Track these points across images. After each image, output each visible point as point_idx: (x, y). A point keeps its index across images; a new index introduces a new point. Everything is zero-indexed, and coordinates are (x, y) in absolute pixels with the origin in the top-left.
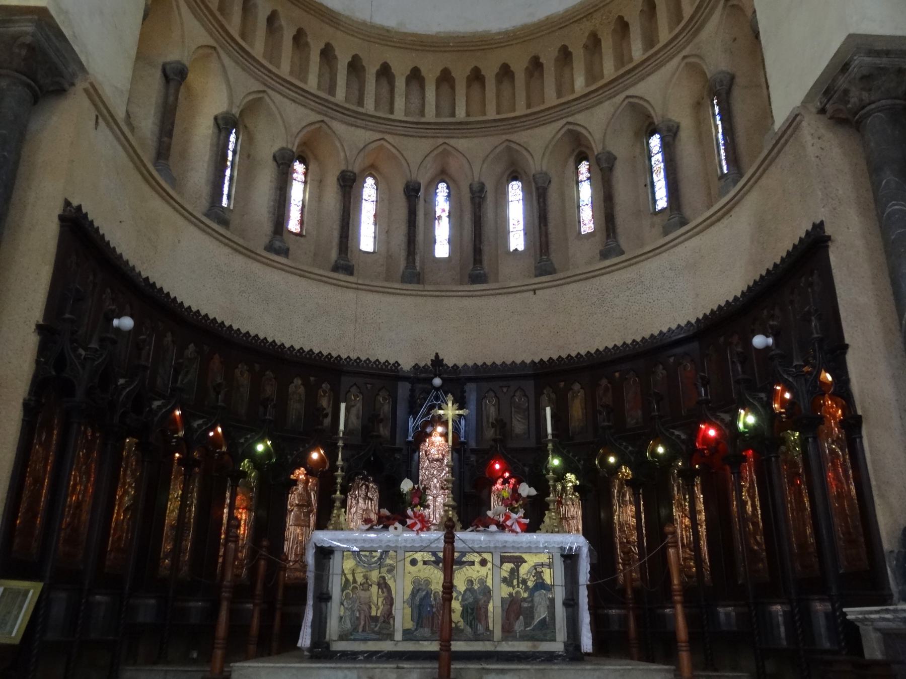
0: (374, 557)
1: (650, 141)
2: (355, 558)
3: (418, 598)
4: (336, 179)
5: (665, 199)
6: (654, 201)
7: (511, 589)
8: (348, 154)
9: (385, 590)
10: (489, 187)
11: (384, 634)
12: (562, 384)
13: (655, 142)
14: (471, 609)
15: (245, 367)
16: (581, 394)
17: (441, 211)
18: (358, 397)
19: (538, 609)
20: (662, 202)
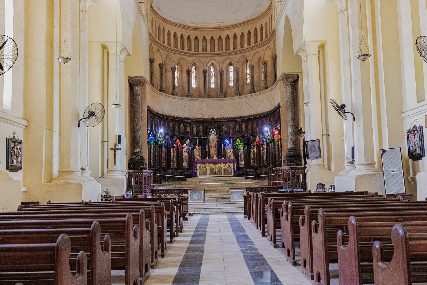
8: (188, 64)
10: (224, 69)
16: (245, 125)
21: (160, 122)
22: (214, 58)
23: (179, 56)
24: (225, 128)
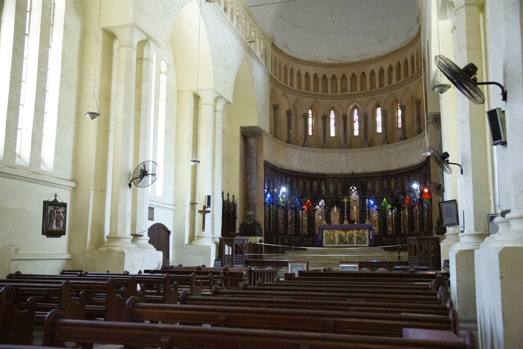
3: (340, 237)
10: (369, 112)
16: (394, 181)
21: (286, 180)
22: (356, 99)
23: (312, 100)
24: (370, 186)
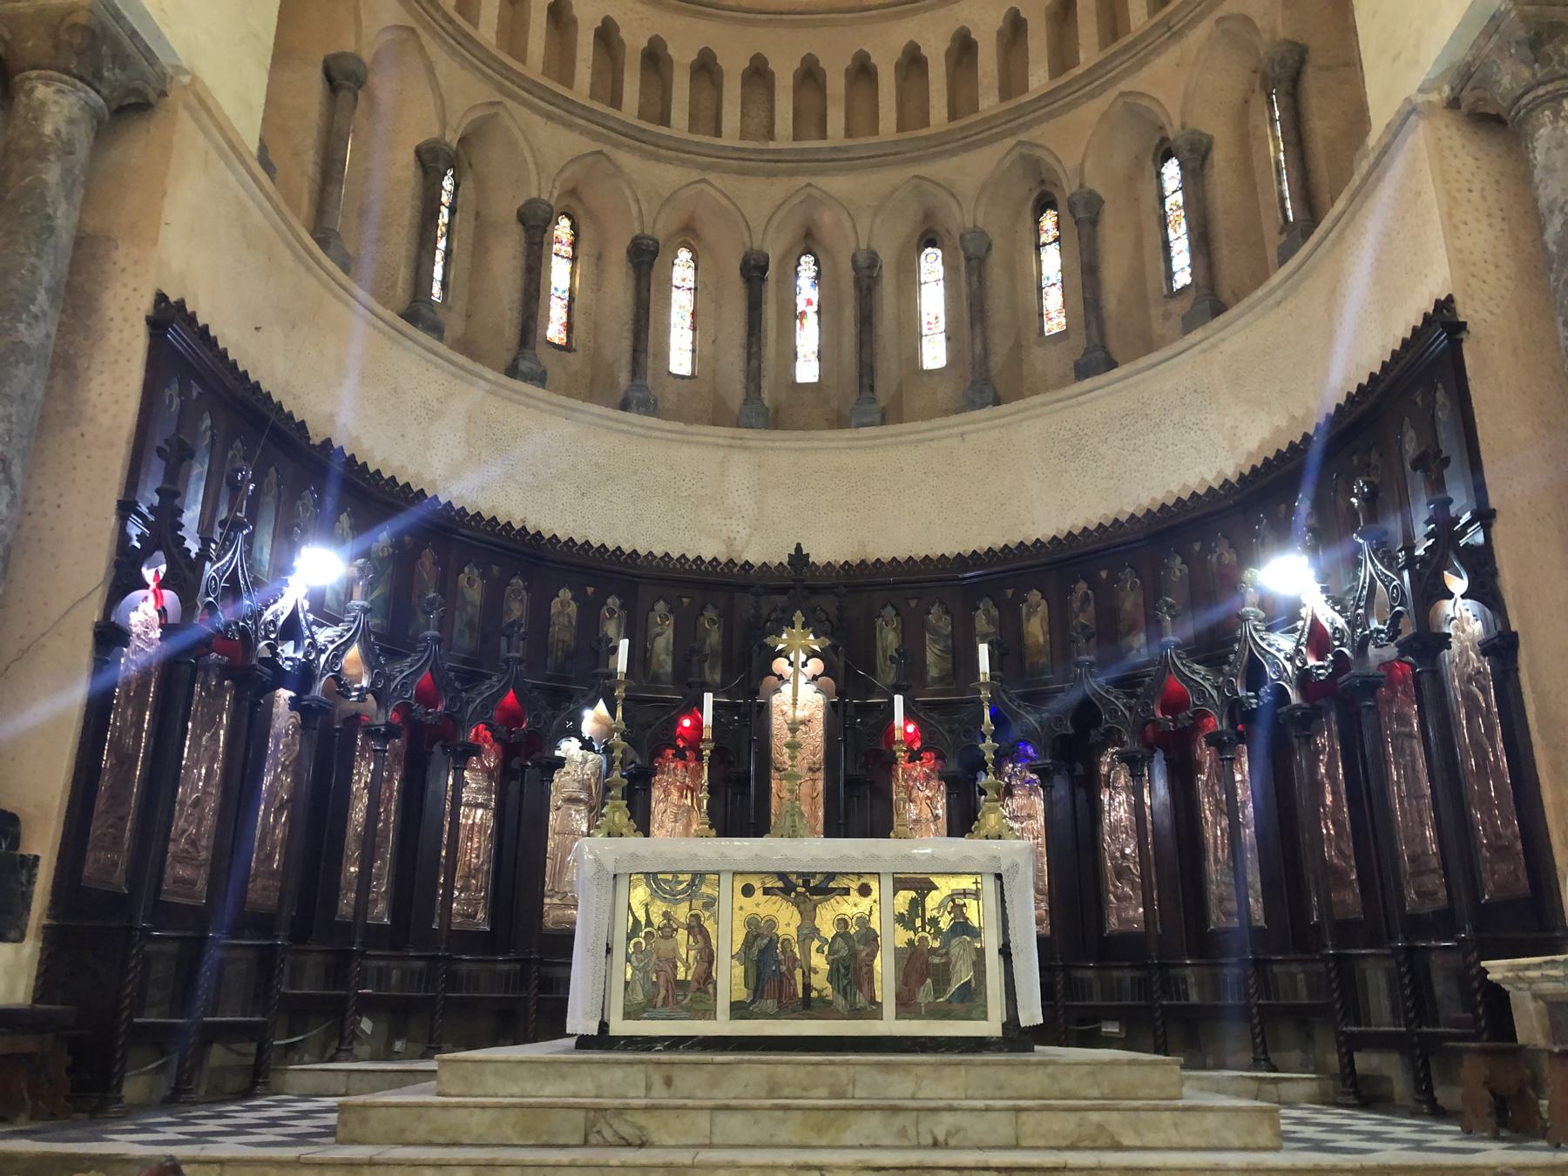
0: (681, 883)
1: (1163, 170)
2: (649, 885)
3: (755, 951)
4: (624, 251)
5: (1189, 270)
6: (1170, 275)
7: (911, 934)
8: (644, 206)
9: (699, 937)
10: (886, 256)
11: (699, 1011)
12: (1010, 592)
13: (1172, 172)
14: (844, 967)
15: (476, 571)
16: (1043, 608)
17: (805, 303)
18: (668, 619)
19: (958, 967)
20: (1182, 278)
23: (585, 145)
